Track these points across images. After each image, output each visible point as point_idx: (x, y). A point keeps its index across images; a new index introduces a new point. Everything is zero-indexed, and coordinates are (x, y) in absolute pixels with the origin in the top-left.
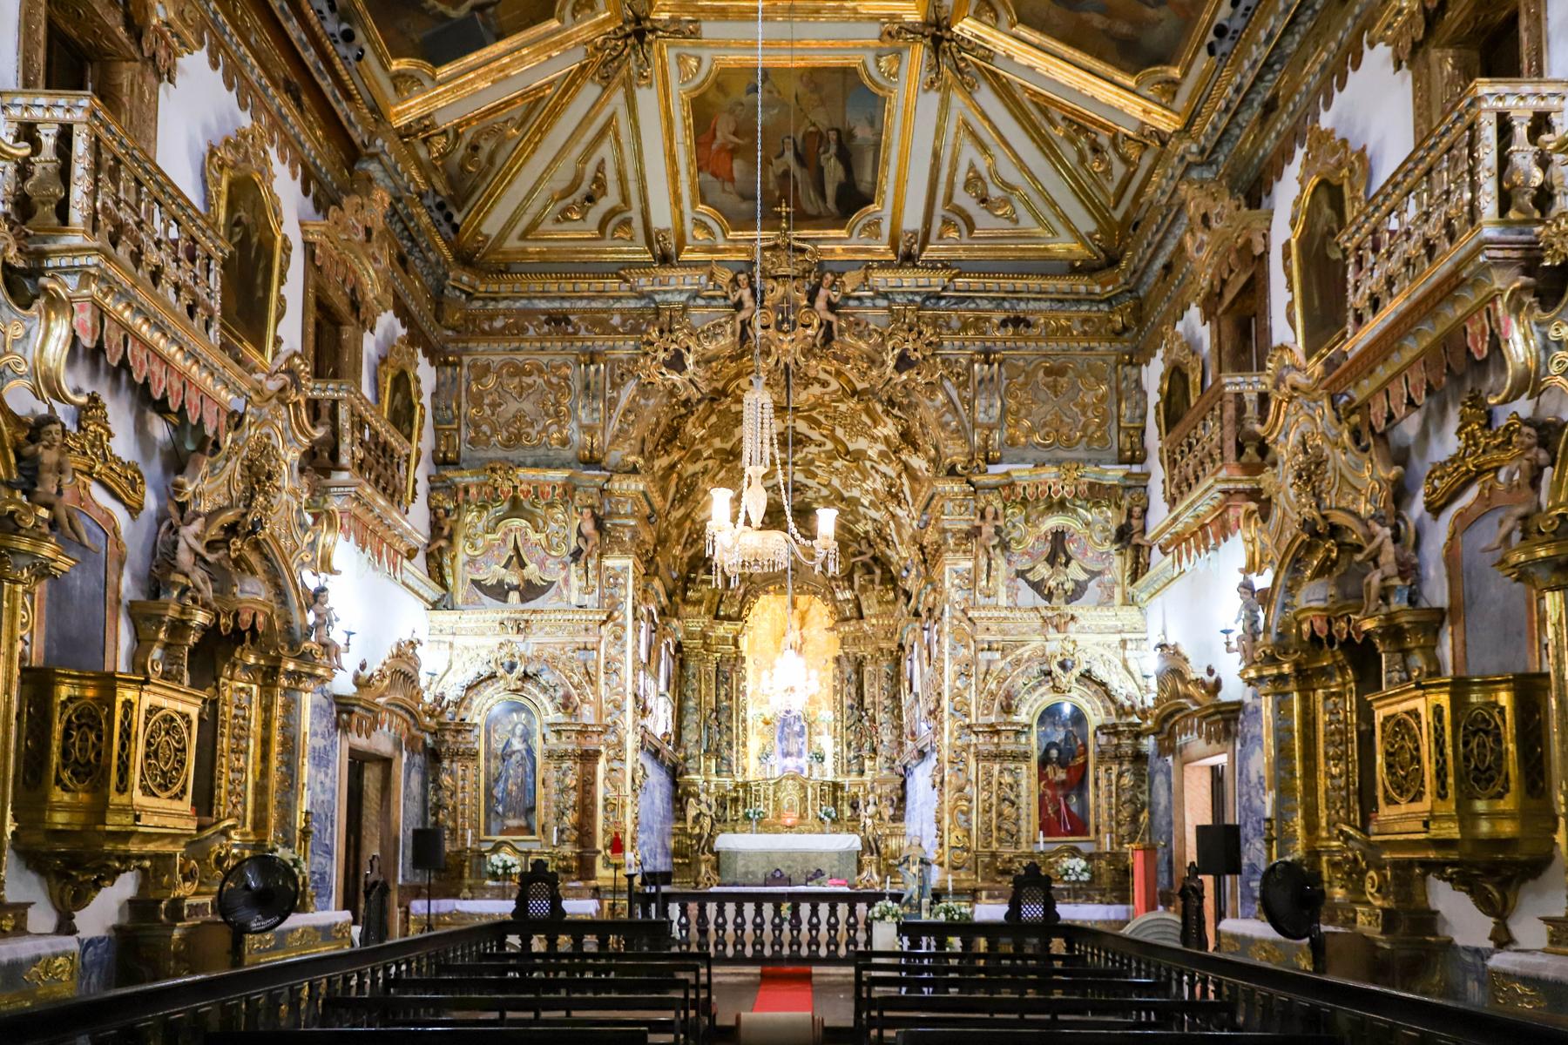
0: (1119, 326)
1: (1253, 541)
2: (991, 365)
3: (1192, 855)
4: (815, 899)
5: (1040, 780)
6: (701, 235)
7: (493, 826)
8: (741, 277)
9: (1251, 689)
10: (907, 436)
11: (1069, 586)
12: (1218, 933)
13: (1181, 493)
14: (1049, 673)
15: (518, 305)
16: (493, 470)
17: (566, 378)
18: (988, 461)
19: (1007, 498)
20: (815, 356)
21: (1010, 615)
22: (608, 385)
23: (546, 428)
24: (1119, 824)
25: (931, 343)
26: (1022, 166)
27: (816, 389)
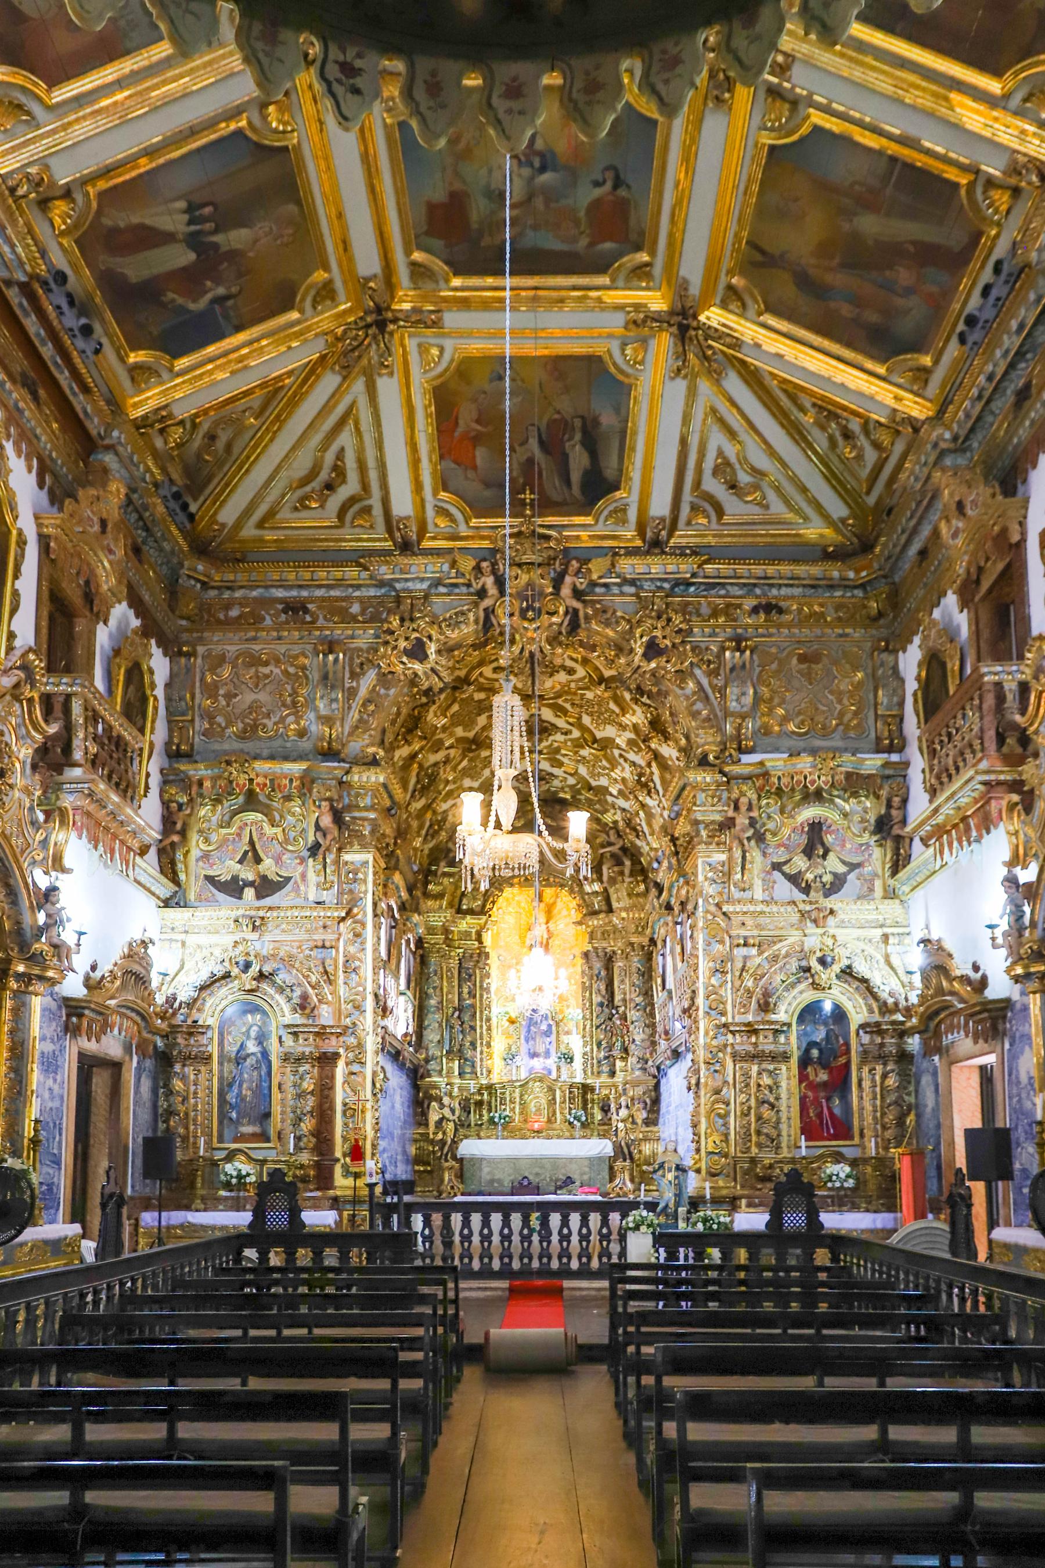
1: (1016, 833)
2: (743, 652)
3: (961, 1161)
4: (565, 1208)
5: (800, 1082)
6: (443, 523)
7: (226, 1132)
8: (484, 564)
9: (1018, 986)
10: (657, 725)
11: (827, 878)
12: (990, 1242)
13: (941, 783)
14: (808, 970)
15: (255, 593)
16: (229, 763)
17: (304, 668)
18: (741, 750)
19: (761, 789)
20: (560, 644)
21: (767, 909)
22: (347, 675)
23: (283, 719)
24: (884, 1128)
25: (680, 631)
26: (771, 452)
27: (562, 677)
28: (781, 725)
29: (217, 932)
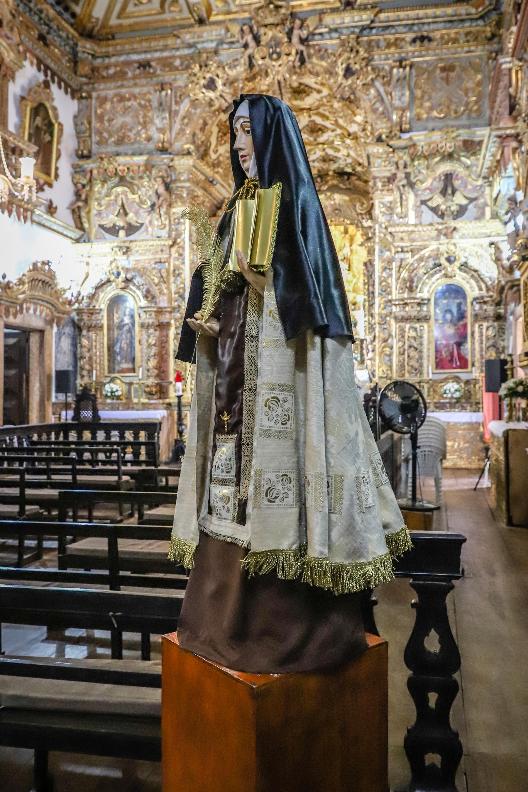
0: (489, 35)
2: (404, 68)
18: (401, 131)
23: (139, 132)
28: (428, 113)
29: (106, 256)
